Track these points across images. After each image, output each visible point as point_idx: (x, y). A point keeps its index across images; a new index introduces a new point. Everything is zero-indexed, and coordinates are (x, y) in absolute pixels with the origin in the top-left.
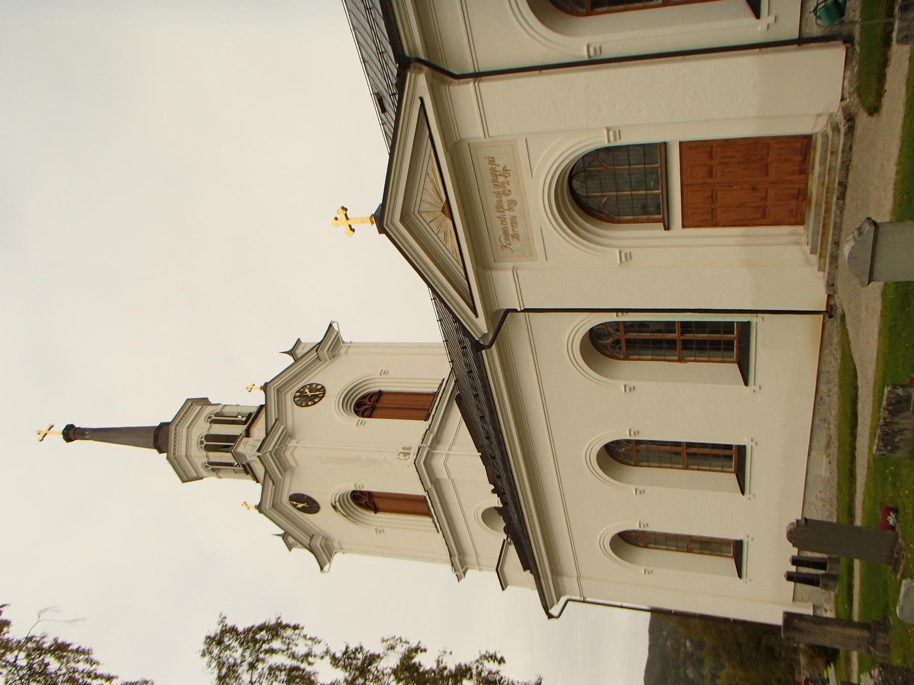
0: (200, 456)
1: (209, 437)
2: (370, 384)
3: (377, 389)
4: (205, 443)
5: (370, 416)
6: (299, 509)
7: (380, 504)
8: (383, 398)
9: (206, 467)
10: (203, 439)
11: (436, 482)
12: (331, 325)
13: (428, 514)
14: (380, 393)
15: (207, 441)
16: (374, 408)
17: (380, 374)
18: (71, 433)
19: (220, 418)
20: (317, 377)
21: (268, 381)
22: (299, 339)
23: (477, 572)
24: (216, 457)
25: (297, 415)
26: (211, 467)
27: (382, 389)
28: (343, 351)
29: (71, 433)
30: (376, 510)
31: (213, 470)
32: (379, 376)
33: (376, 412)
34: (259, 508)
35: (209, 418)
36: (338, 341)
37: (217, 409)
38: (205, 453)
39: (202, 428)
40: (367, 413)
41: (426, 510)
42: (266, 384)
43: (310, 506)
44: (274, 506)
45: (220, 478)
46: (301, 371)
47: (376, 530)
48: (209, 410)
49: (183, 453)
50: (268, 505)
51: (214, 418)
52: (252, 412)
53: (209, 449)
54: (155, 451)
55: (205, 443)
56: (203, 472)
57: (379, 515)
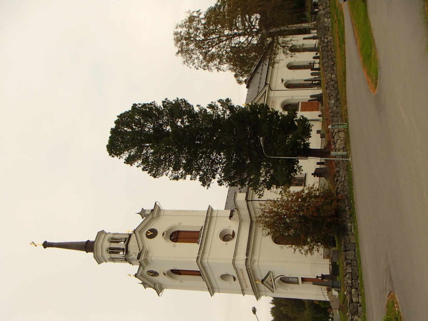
0: (107, 256)
1: (110, 248)
2: (174, 228)
3: (178, 230)
4: (109, 251)
5: (176, 242)
6: (151, 275)
7: (181, 272)
8: (180, 234)
9: (109, 259)
10: (108, 249)
11: (204, 267)
12: (156, 203)
13: (201, 275)
14: (179, 232)
15: (110, 250)
16: (177, 238)
17: (179, 224)
18: (46, 245)
19: (114, 240)
20: (154, 226)
21: (135, 229)
22: (143, 208)
23: (218, 293)
24: (113, 255)
25: (149, 243)
26: (111, 259)
27: (179, 230)
28: (162, 213)
29: (46, 245)
30: (180, 274)
31: (112, 260)
32: (178, 225)
33: (178, 240)
34: (136, 276)
35: (109, 240)
36: (159, 209)
37: (111, 236)
38: (110, 254)
39: (107, 245)
40: (175, 240)
41: (199, 274)
42: (135, 230)
43: (155, 274)
44: (141, 275)
45: (114, 262)
46: (147, 224)
47: (180, 281)
48: (108, 237)
49: (100, 255)
50: (139, 274)
51: (111, 240)
52: (126, 237)
53: (110, 253)
54: (85, 252)
55: (109, 251)
56: (107, 260)
57: (181, 276)
